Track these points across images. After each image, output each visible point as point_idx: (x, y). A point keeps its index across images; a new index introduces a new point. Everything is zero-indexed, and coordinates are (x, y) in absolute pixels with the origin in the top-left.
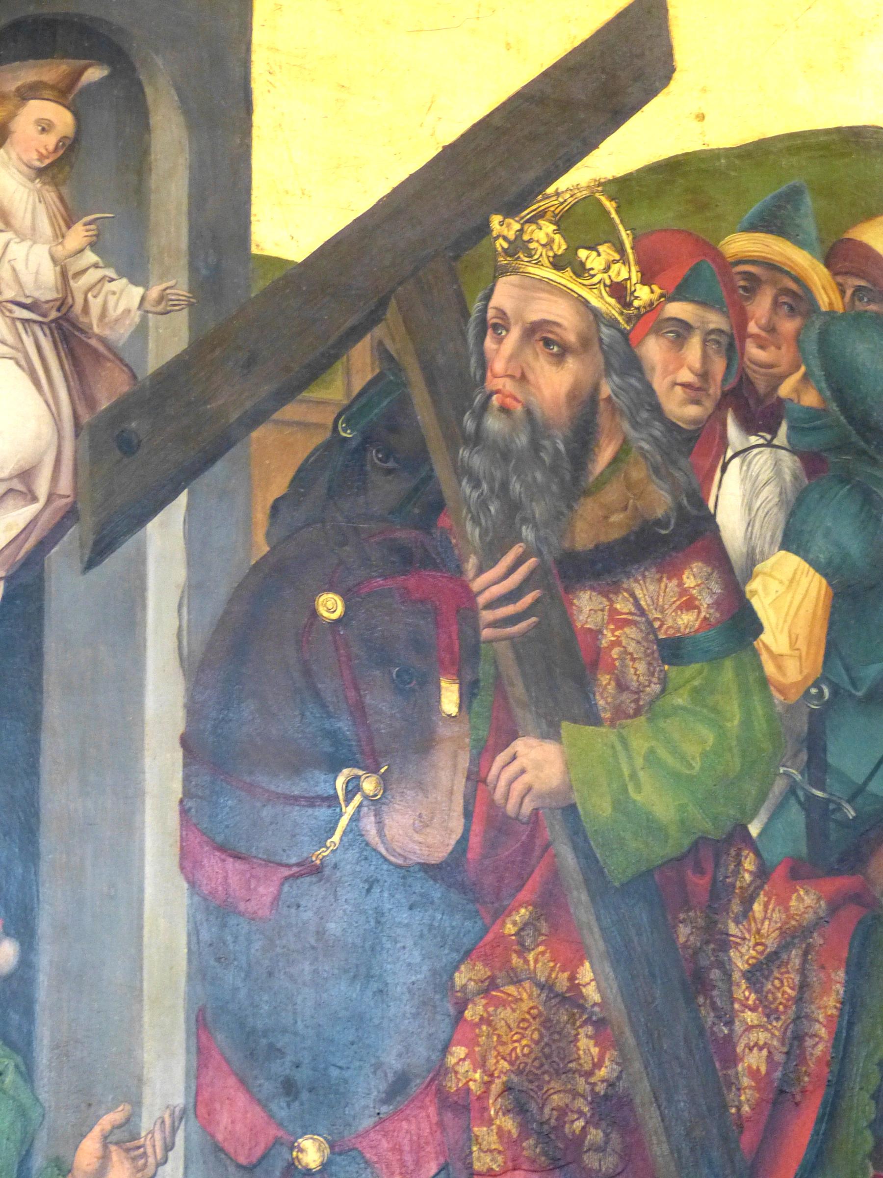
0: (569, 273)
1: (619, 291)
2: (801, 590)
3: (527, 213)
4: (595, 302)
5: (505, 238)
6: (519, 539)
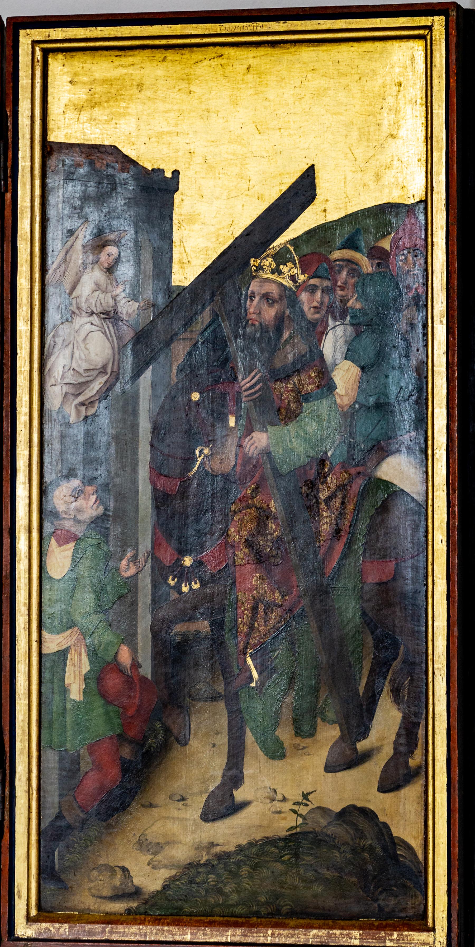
0: (276, 274)
1: (293, 278)
2: (351, 373)
3: (263, 256)
4: (284, 283)
5: (255, 266)
6: (256, 367)
